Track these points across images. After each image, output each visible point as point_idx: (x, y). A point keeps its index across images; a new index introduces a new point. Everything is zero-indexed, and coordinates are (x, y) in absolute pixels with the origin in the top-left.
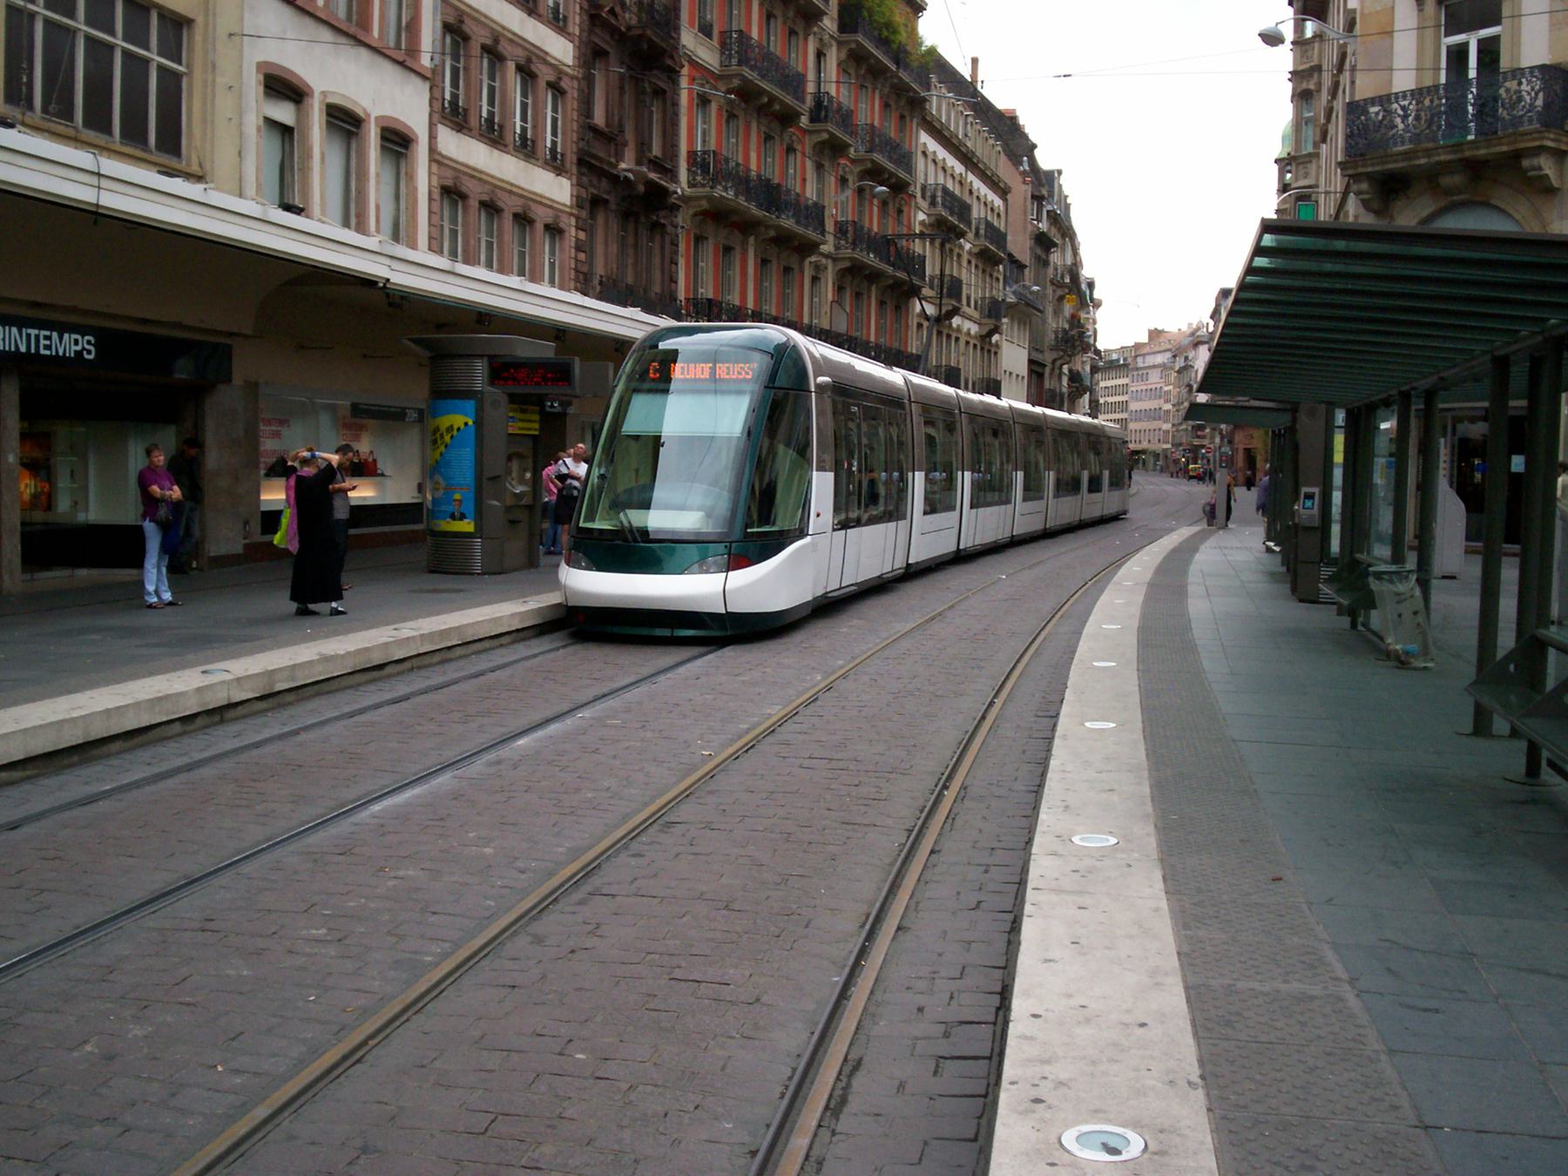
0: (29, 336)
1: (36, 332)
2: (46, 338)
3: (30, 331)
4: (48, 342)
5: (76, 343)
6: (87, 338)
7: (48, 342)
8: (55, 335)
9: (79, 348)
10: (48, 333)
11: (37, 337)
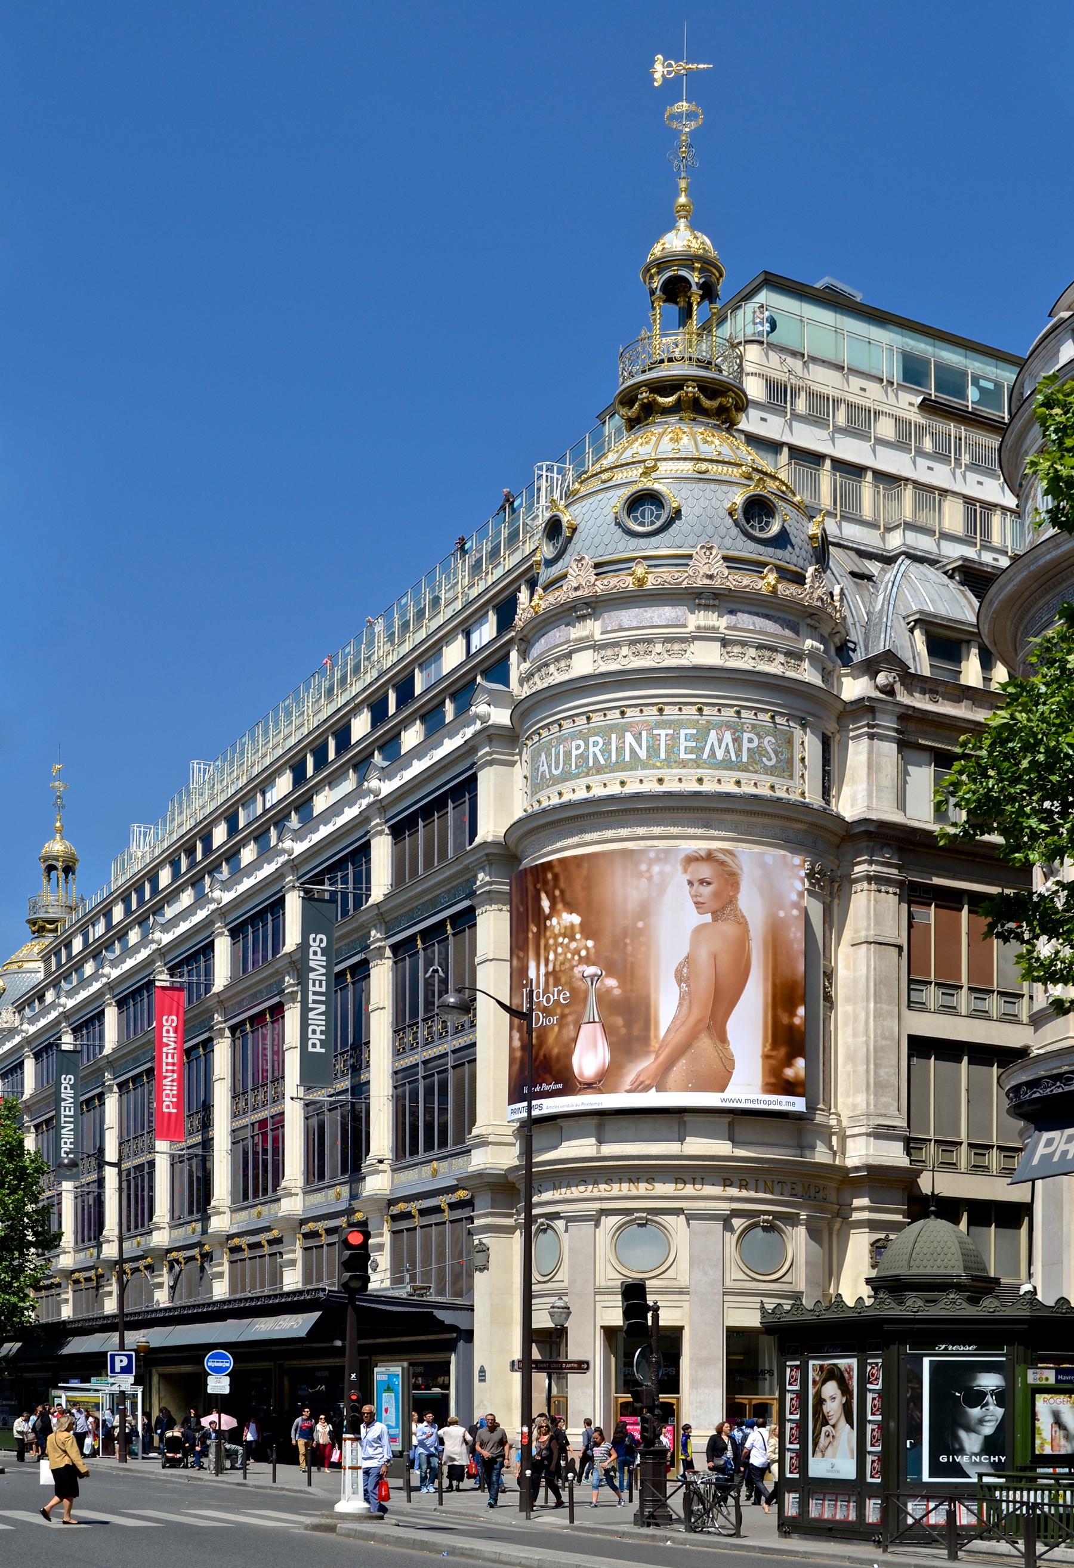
0: (314, 1002)
1: (310, 993)
2: (314, 985)
3: (310, 1001)
4: (317, 983)
5: (315, 953)
6: (311, 942)
7: (317, 983)
8: (312, 975)
9: (319, 951)
10: (311, 982)
11: (315, 993)
